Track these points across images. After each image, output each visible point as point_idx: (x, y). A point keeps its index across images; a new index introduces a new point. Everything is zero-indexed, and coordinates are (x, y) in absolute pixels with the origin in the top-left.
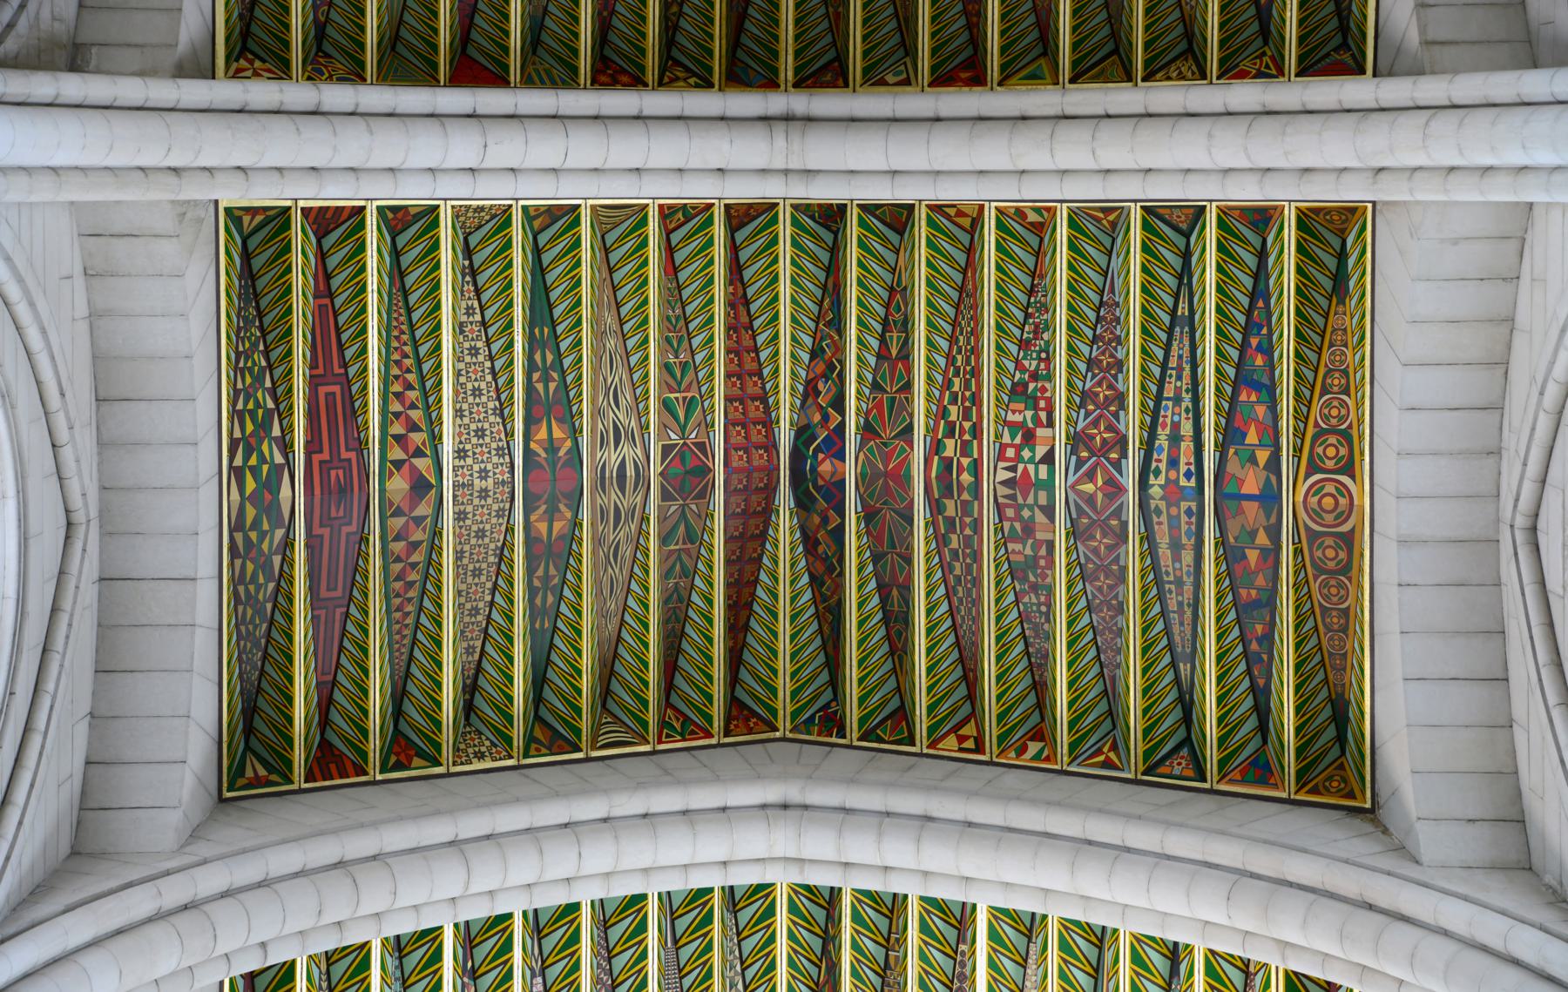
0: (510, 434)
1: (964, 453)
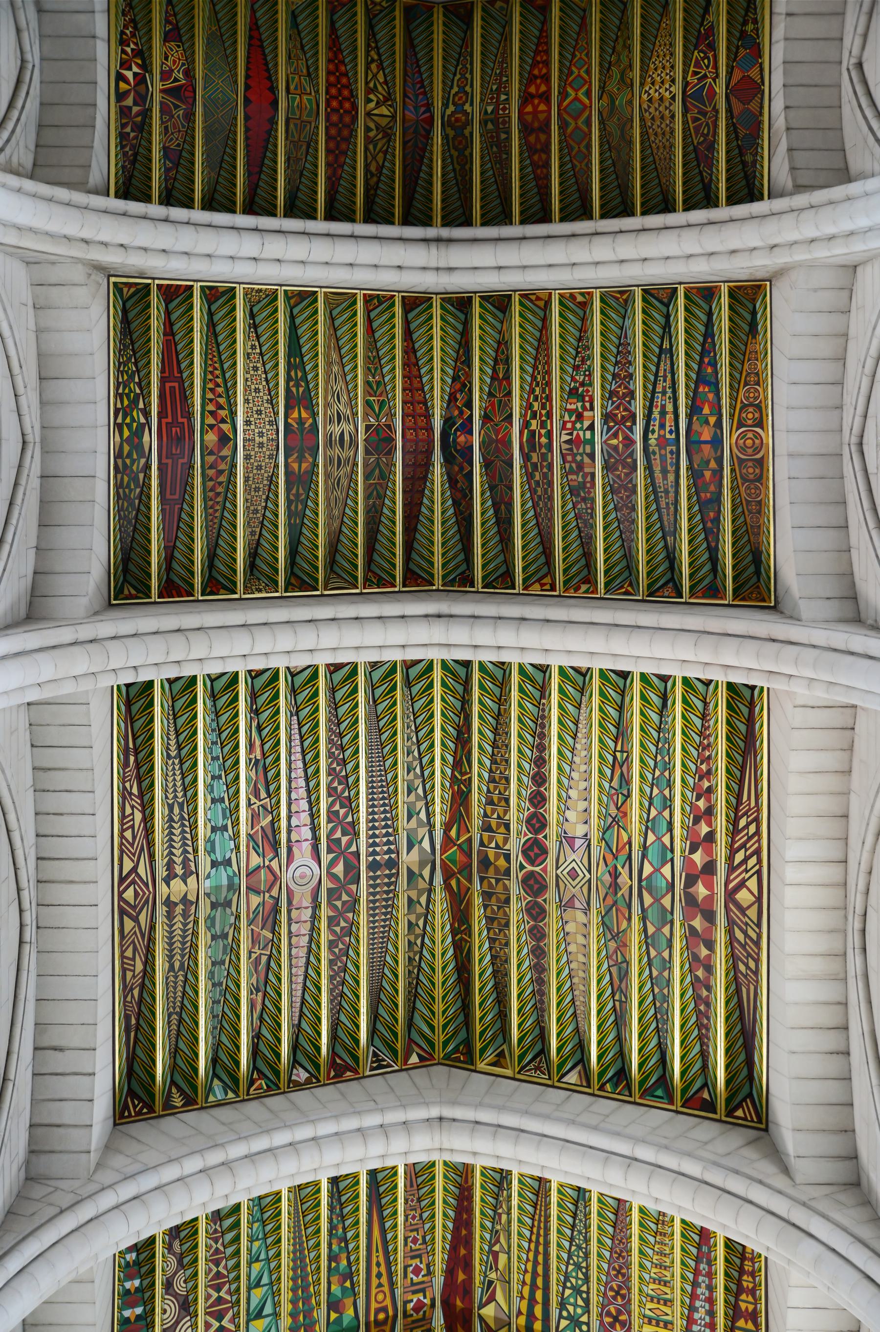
0: (276, 414)
1: (543, 427)
